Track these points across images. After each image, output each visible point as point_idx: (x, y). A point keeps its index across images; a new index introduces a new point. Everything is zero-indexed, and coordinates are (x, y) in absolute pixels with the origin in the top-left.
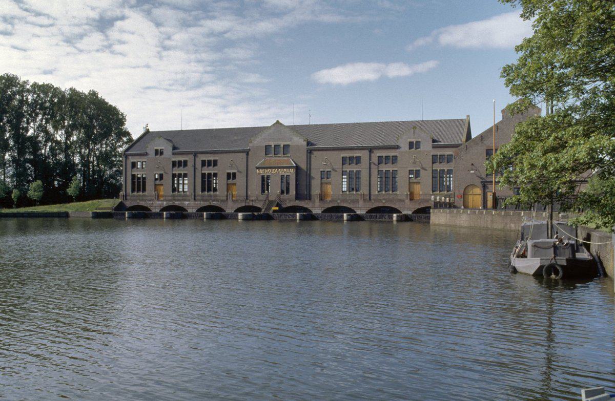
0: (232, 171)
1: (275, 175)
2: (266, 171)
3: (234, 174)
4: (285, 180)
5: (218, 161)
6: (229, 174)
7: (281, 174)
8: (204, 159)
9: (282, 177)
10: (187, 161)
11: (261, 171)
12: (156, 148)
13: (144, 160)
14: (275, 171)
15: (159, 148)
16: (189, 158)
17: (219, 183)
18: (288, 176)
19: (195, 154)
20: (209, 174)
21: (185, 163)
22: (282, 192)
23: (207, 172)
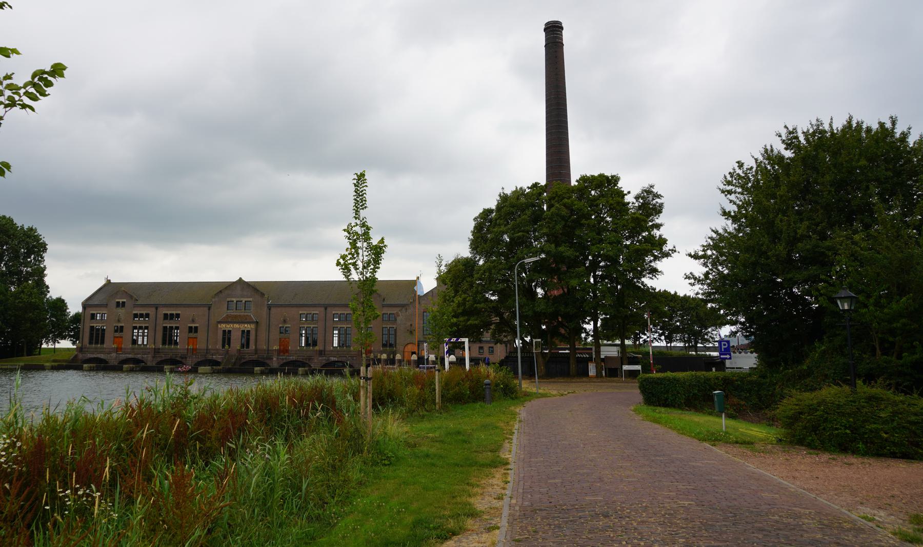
0: (193, 325)
1: (236, 328)
2: (228, 326)
3: (196, 328)
4: (246, 334)
5: (180, 315)
6: (190, 328)
7: (241, 329)
8: (166, 312)
9: (243, 331)
10: (149, 314)
11: (223, 326)
12: (117, 300)
13: (104, 312)
14: (236, 326)
15: (121, 301)
16: (151, 311)
17: (179, 336)
18: (248, 332)
19: (157, 307)
20: (171, 328)
21: (147, 315)
22: (243, 346)
23: (168, 326)
